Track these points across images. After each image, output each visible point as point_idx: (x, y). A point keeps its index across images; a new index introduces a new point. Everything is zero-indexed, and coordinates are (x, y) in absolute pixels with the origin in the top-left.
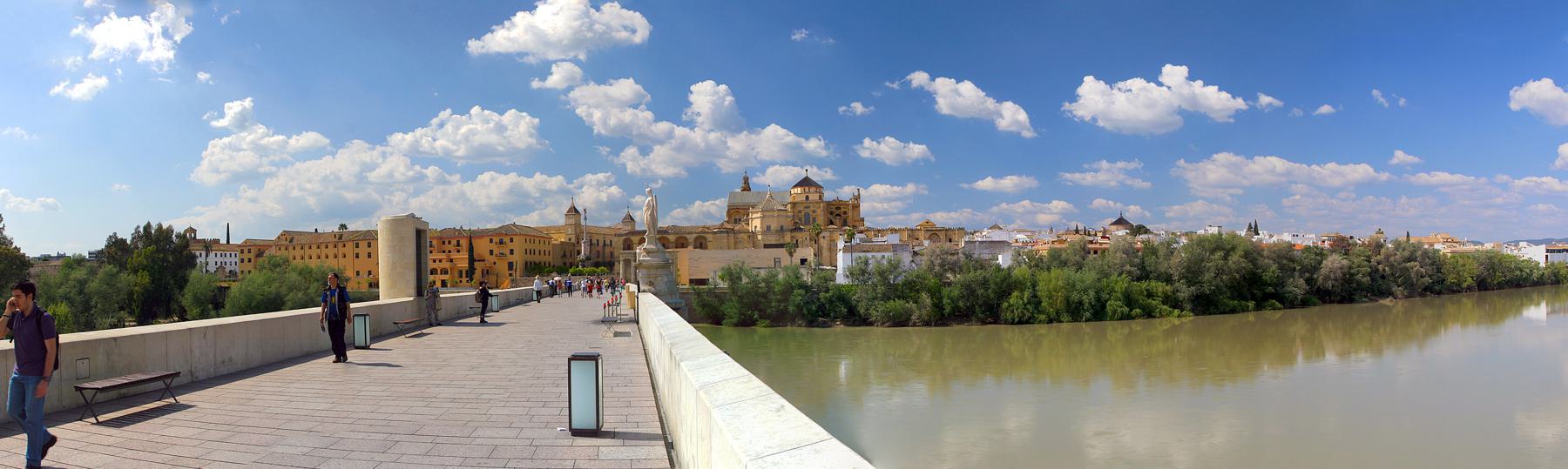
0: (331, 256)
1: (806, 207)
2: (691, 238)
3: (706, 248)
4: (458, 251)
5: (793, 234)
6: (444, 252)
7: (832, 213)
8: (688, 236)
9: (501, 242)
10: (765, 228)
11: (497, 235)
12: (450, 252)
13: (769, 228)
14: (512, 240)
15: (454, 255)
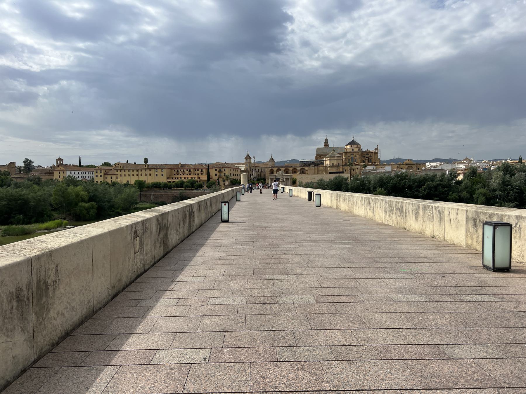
0: (144, 175)
1: (352, 154)
2: (299, 169)
3: (305, 173)
4: (202, 174)
5: (343, 167)
6: (196, 174)
7: (364, 157)
8: (297, 168)
9: (220, 171)
10: (331, 164)
11: (219, 168)
12: (198, 174)
13: (333, 164)
14: (225, 170)
15: (200, 176)
